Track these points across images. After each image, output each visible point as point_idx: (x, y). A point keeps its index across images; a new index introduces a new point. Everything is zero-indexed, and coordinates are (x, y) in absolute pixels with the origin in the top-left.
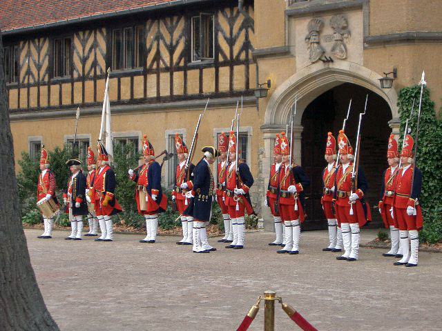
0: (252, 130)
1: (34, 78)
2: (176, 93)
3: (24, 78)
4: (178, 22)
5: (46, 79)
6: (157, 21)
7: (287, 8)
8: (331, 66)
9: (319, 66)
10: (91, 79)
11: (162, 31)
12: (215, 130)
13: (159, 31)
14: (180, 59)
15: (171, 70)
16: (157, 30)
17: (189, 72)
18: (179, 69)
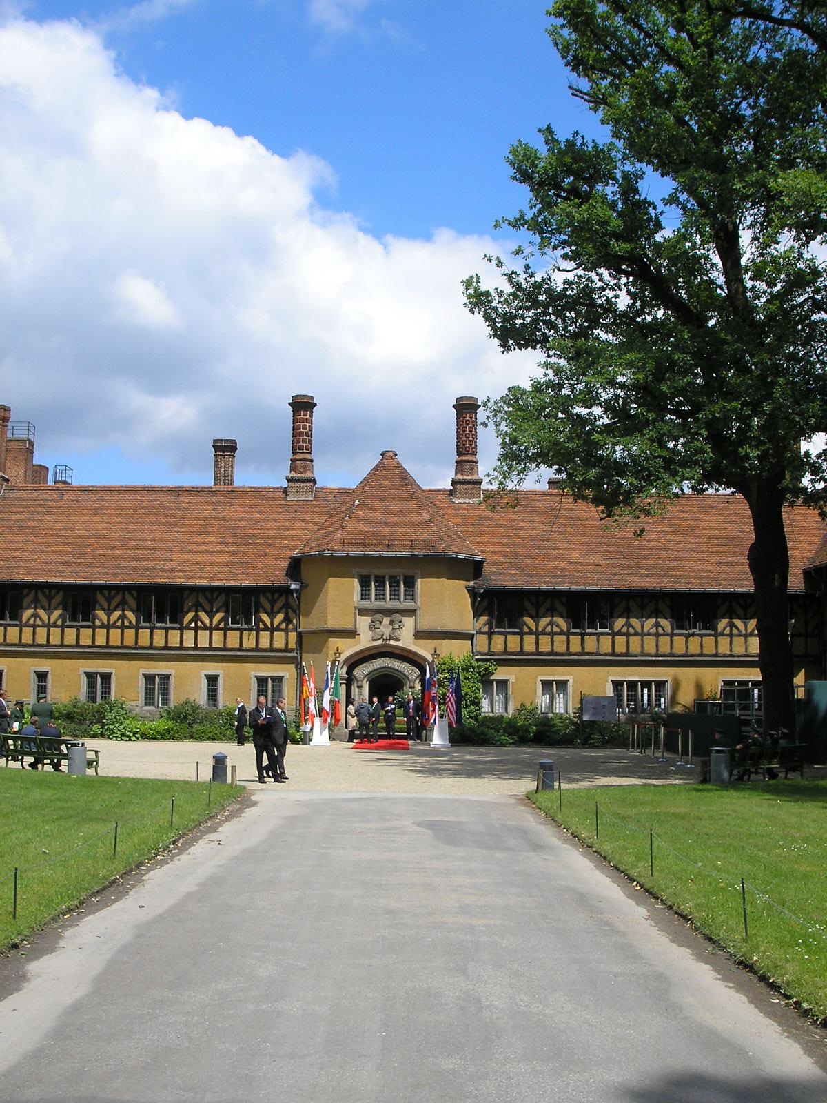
0: (288, 674)
1: (41, 619)
2: (214, 645)
3: (29, 619)
4: (217, 598)
5: (59, 623)
6: (195, 593)
7: (356, 605)
8: (388, 642)
9: (380, 642)
10: (118, 627)
11: (201, 600)
12: (253, 674)
13: (198, 600)
14: (220, 622)
15: (211, 629)
16: (195, 599)
17: (228, 632)
18: (217, 628)
